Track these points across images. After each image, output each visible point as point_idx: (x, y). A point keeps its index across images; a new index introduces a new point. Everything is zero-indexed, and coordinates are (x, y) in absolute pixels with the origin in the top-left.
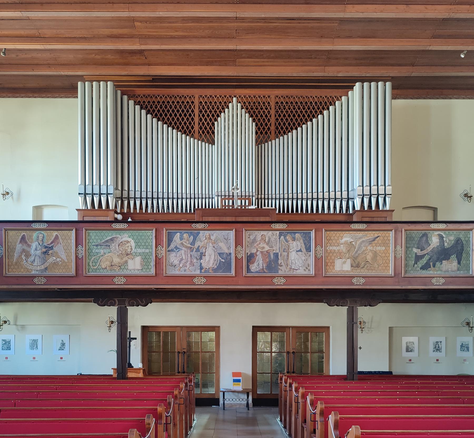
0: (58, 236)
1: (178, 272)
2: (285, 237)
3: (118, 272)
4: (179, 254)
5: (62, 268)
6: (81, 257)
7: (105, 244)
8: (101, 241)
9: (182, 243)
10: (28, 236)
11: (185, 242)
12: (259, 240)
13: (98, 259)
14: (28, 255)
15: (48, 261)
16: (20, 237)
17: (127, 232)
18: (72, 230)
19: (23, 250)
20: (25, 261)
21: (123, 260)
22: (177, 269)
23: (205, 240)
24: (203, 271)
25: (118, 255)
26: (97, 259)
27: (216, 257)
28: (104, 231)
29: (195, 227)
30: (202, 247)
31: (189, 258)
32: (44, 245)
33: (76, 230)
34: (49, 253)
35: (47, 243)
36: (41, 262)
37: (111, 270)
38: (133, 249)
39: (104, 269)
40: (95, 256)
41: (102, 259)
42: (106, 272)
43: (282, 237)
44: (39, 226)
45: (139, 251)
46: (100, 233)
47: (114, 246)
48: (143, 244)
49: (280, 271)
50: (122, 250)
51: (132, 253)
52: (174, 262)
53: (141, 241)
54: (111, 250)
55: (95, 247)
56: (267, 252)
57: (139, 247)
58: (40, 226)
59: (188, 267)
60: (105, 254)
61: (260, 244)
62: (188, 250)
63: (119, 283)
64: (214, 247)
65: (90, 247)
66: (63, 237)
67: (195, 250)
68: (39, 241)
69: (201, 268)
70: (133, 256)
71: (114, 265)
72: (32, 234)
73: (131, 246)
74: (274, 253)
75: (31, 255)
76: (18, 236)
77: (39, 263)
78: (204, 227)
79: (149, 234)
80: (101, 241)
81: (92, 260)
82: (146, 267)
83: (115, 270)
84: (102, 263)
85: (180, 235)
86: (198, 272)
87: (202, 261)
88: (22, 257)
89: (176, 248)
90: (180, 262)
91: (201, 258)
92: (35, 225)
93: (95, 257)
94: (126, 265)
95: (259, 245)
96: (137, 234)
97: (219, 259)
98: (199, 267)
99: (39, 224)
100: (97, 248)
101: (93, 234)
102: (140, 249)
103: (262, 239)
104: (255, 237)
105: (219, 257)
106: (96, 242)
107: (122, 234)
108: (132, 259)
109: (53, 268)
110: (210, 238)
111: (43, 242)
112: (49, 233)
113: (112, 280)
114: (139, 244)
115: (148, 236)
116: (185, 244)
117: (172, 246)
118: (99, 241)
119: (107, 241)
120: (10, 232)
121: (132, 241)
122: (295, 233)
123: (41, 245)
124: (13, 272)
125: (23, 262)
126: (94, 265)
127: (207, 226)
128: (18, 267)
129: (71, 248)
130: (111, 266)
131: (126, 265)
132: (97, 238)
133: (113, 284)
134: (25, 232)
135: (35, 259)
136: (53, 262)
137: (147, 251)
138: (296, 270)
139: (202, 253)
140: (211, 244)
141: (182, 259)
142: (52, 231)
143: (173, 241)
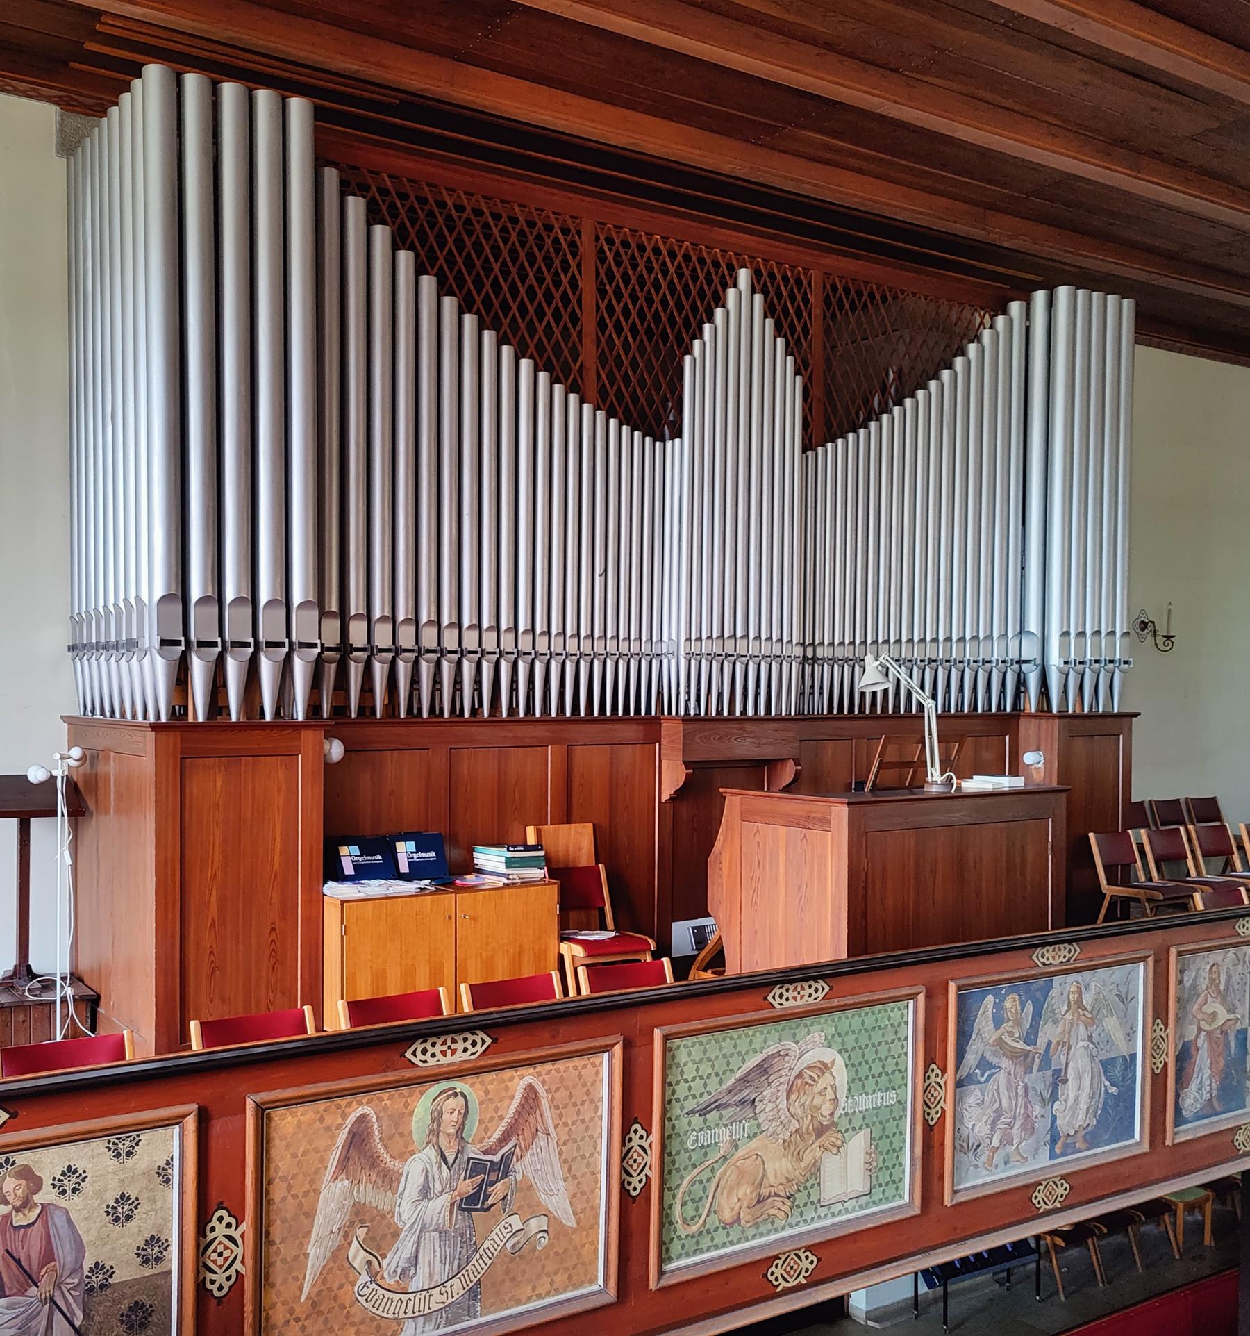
0: (536, 1092)
3: (783, 1228)
6: (639, 1186)
7: (737, 1098)
8: (721, 1082)
9: (1000, 1042)
10: (385, 1123)
11: (1008, 1032)
12: (1204, 987)
13: (709, 1180)
14: (384, 1237)
15: (485, 1246)
16: (342, 1137)
17: (822, 1020)
18: (608, 1048)
19: (357, 1213)
20: (365, 1278)
21: (803, 1165)
22: (984, 1158)
23: (1067, 1012)
25: (785, 1141)
26: (701, 1182)
28: (734, 1034)
29: (1044, 964)
30: (1058, 1043)
32: (465, 1159)
33: (627, 1046)
34: (490, 1201)
35: (481, 1141)
36: (451, 1263)
37: (757, 1225)
38: (842, 1100)
39: (731, 1224)
40: (694, 1166)
41: (724, 1173)
42: (739, 1242)
44: (444, 1053)
45: (865, 1102)
46: (717, 1041)
47: (771, 1098)
48: (877, 1068)
50: (799, 1111)
51: (836, 1119)
52: (976, 1130)
53: (870, 1055)
54: (760, 1121)
55: (697, 1120)
57: (864, 1086)
59: (1016, 1141)
60: (736, 1147)
62: (1018, 1067)
63: (792, 1283)
64: (1090, 1039)
65: (676, 1122)
66: (563, 1094)
67: (1037, 1061)
68: (443, 1141)
69: (1054, 1141)
70: (840, 1136)
72: (406, 1105)
73: (834, 1087)
75: (396, 1235)
76: (328, 1129)
77: (438, 1265)
78: (1068, 956)
79: (892, 1013)
80: (721, 1082)
81: (681, 1190)
82: (884, 1177)
83: (773, 1223)
85: (995, 1003)
86: (1043, 1161)
88: (351, 1255)
89: (984, 1064)
90: (994, 1124)
91: (1054, 1097)
92: (424, 1052)
93: (697, 1171)
95: (1204, 1008)
97: (1103, 1089)
98: (1048, 1136)
99: (444, 1043)
100: (705, 1121)
101: (689, 1052)
102: (867, 1094)
103: (1212, 980)
104: (1195, 979)
105: (1103, 1078)
106: (702, 1094)
107: (801, 1031)
108: (835, 1150)
109: (507, 1283)
110: (1080, 1006)
111: (462, 1138)
112: (492, 1082)
113: (765, 1275)
115: (892, 1025)
116: (1008, 1040)
117: (971, 1059)
118: (713, 1084)
119: (744, 1080)
120: (283, 1117)
121: (840, 1061)
123: (450, 1160)
126: (692, 1213)
127: (1075, 951)
128: (326, 1322)
129: (595, 1145)
130: (759, 1201)
132: (705, 1069)
133: (767, 1293)
134: (369, 1102)
135: (417, 1251)
136: (509, 1246)
137: (891, 1098)
139: (1057, 1072)
140: (1082, 1028)
141: (999, 1113)
142: (507, 1074)
143: (973, 1038)
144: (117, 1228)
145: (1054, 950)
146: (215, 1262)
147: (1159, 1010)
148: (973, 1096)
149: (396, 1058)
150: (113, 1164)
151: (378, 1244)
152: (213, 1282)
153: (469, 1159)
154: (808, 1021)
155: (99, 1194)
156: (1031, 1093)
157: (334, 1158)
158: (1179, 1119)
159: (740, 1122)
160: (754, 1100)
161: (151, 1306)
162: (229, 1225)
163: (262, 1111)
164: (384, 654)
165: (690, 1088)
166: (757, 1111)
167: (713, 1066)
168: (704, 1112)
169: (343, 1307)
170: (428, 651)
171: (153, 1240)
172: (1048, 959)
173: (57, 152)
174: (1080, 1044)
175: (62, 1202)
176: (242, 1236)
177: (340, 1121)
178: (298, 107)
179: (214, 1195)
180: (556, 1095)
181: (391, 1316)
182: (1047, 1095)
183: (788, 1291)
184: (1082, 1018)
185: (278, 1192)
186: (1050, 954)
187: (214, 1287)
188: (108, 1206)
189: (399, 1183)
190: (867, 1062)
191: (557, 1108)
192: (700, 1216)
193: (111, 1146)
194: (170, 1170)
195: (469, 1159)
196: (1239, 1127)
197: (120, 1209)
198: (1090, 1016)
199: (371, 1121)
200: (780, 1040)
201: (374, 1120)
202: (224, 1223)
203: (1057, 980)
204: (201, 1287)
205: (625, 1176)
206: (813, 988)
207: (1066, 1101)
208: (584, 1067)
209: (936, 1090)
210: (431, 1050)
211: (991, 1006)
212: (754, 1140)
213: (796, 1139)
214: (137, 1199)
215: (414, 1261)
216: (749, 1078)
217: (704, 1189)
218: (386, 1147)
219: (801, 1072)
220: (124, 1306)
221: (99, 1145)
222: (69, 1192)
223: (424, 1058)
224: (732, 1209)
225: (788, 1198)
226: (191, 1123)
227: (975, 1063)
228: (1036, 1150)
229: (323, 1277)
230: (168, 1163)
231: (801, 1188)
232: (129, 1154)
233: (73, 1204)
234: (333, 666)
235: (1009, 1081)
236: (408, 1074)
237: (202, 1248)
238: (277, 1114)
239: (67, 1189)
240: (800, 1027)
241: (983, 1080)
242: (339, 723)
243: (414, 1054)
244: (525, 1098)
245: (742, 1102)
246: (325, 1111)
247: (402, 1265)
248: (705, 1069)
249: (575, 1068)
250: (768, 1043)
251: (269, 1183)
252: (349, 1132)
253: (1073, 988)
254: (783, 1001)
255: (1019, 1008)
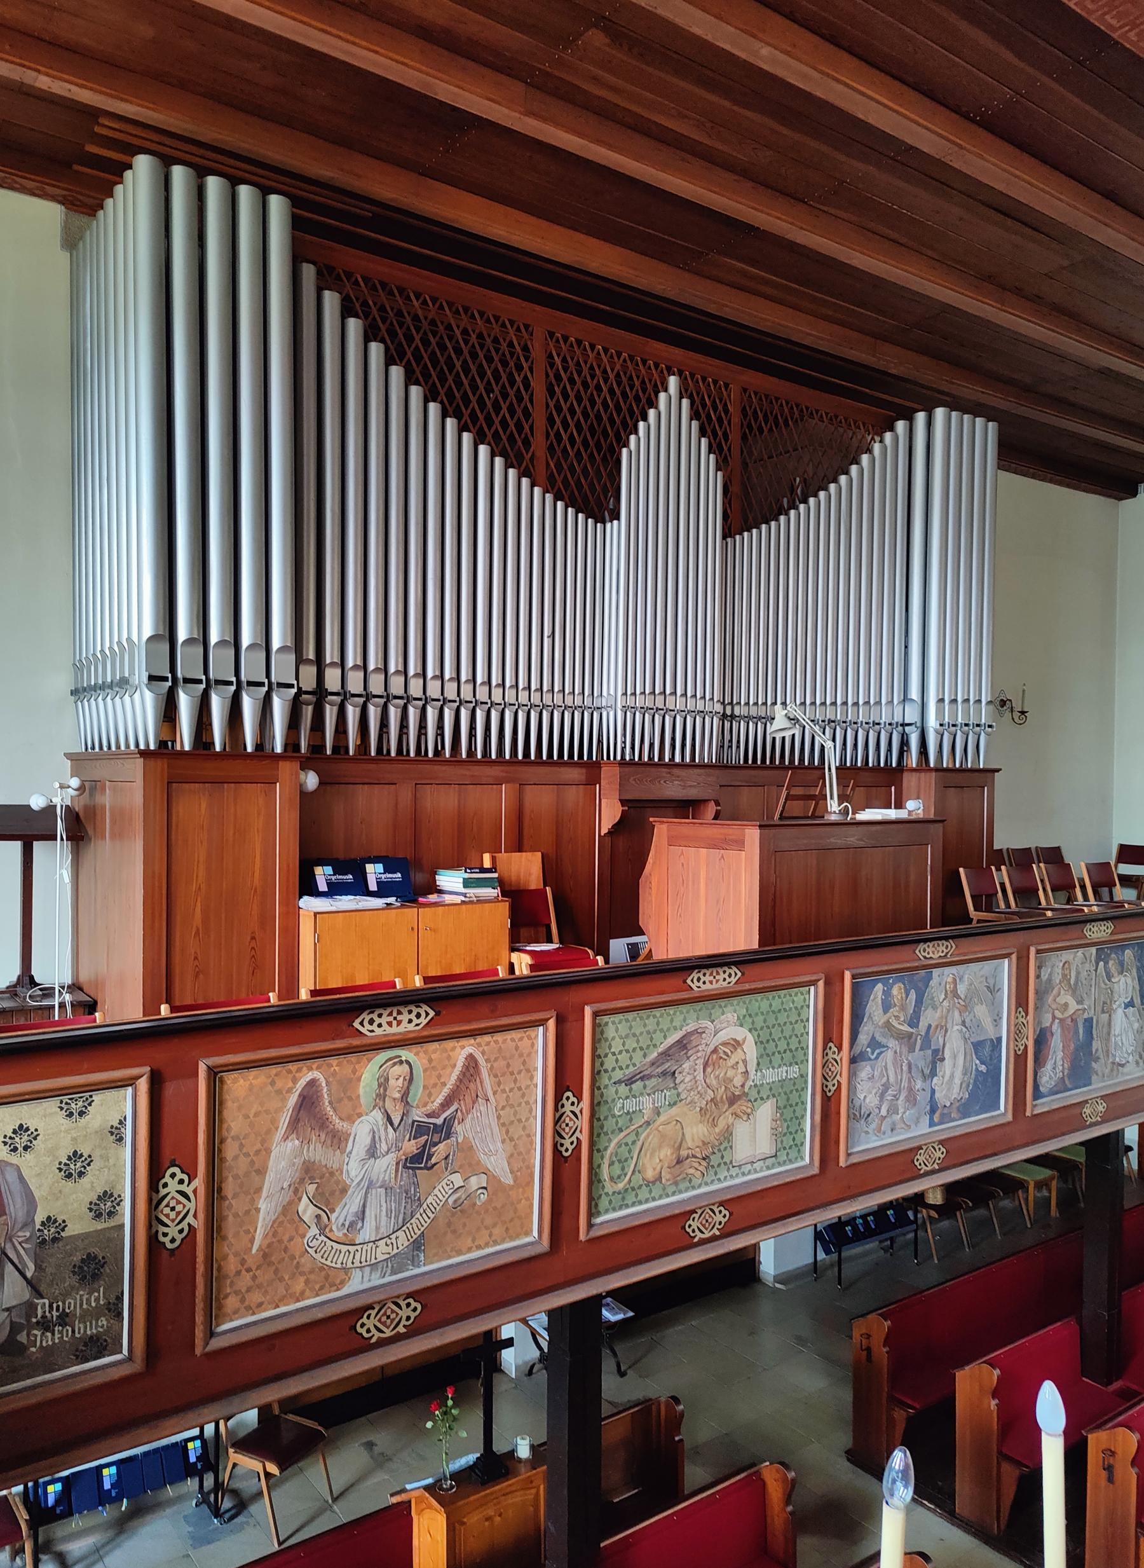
1: (876, 1138)
2: (1106, 963)
3: (700, 1186)
4: (880, 1063)
5: (489, 1221)
6: (571, 1148)
7: (660, 1070)
9: (888, 1024)
12: (1058, 982)
13: (634, 1142)
14: (332, 1193)
15: (429, 1201)
16: (293, 1099)
17: (735, 1002)
18: (543, 1022)
20: (314, 1231)
21: (717, 1130)
22: (874, 1126)
24: (936, 1118)
25: (701, 1109)
26: (626, 1144)
27: (968, 1057)
28: (657, 1012)
29: (925, 957)
30: (937, 1026)
31: (904, 1076)
32: (410, 1121)
33: (560, 1022)
34: (433, 1160)
35: (425, 1105)
36: (397, 1217)
37: (676, 1183)
38: (752, 1072)
39: (654, 1183)
40: (621, 1130)
41: (648, 1136)
42: (660, 1197)
43: (1101, 964)
44: (390, 1024)
45: (771, 1075)
46: (641, 1018)
47: (690, 1070)
48: (782, 1045)
49: (1094, 1077)
50: (714, 1082)
51: (746, 1090)
52: (867, 1100)
54: (680, 1090)
55: (623, 1089)
56: (1072, 1020)
57: (771, 1061)
58: (399, 1023)
59: (901, 1111)
60: (659, 1114)
61: (1059, 994)
63: (707, 1235)
64: (963, 1023)
65: (604, 1091)
66: (502, 1063)
67: (919, 1042)
68: (389, 1104)
69: (933, 1111)
70: (750, 1105)
71: (688, 1157)
72: (354, 1072)
73: (745, 1062)
74: (1086, 1020)
75: (344, 1191)
76: (279, 1092)
77: (384, 1218)
78: (945, 951)
79: (796, 997)
80: (645, 1056)
81: (609, 1152)
82: (788, 1141)
83: (690, 1181)
84: (645, 1160)
86: (924, 1128)
87: (935, 1079)
89: (874, 1044)
90: (882, 1096)
91: (933, 1073)
92: (371, 1022)
93: (622, 1135)
94: (725, 1149)
96: (765, 1005)
98: (928, 1108)
99: (390, 1014)
100: (631, 1090)
101: (616, 1028)
102: (773, 1068)
103: (1064, 976)
104: (1050, 974)
106: (628, 1066)
107: (716, 1012)
108: (745, 1118)
111: (407, 1102)
112: (435, 1052)
113: (684, 1228)
114: (771, 1047)
115: (796, 1008)
116: (895, 1023)
117: (863, 1039)
118: (638, 1057)
119: (666, 1055)
120: (235, 1081)
121: (750, 1039)
122: (1123, 948)
124: (248, 1308)
125: (303, 1236)
126: (618, 1172)
128: (276, 1271)
129: (531, 1111)
130: (679, 1162)
131: (725, 1149)
132: (631, 1044)
134: (317, 1068)
135: (364, 1206)
136: (451, 1201)
137: (793, 1073)
138: (1122, 1066)
139: (936, 1052)
140: (956, 1013)
141: (886, 1087)
142: (449, 1044)
143: (865, 1020)
144: (70, 1184)
145: (934, 946)
146: (167, 1216)
147: (1021, 1001)
148: (865, 1071)
149: (344, 1027)
150: (66, 1123)
151: (327, 1200)
152: (165, 1235)
153: (414, 1121)
154: (722, 1002)
155: (51, 1152)
156: (914, 1070)
157: (284, 1120)
158: (1037, 1095)
159: (662, 1091)
160: (674, 1072)
161: (103, 1258)
162: (181, 1182)
163: (214, 1074)
164: (356, 699)
165: (617, 1061)
166: (677, 1081)
167: (638, 1041)
168: (629, 1081)
169: (293, 1257)
170: (396, 697)
171: (106, 1196)
172: (928, 953)
173: (62, 246)
174: (956, 1028)
175: (14, 1159)
176: (195, 1192)
177: (290, 1084)
178: (276, 202)
179: (167, 1153)
180: (495, 1065)
181: (339, 1266)
182: (927, 1071)
183: (703, 1242)
184: (958, 1005)
185: (230, 1150)
186: (930, 950)
187: (166, 1240)
188: (60, 1163)
189: (347, 1143)
190: (774, 1040)
191: (496, 1076)
192: (625, 1175)
193: (63, 1105)
194: (123, 1130)
195: (414, 1121)
196: (1086, 1102)
197: (72, 1166)
198: (963, 1003)
199: (320, 1085)
200: (698, 1019)
201: (324, 1084)
202: (177, 1179)
203: (936, 972)
204: (153, 1242)
205: (557, 1138)
206: (727, 973)
207: (943, 1077)
208: (521, 1039)
209: (833, 1065)
210: (377, 1021)
211: (880, 994)
212: (674, 1108)
213: (711, 1107)
214: (90, 1156)
215: (362, 1215)
216: (671, 1052)
217: (630, 1151)
218: (335, 1110)
219: (716, 1048)
220: (77, 1258)
221: (52, 1105)
222: (20, 1149)
223: (371, 1028)
224: (654, 1169)
225: (704, 1159)
226: (143, 1084)
227: (866, 1043)
228: (918, 1119)
229: (274, 1231)
230: (121, 1123)
231: (716, 1151)
232: (81, 1114)
233: (26, 1162)
234: (310, 708)
235: (895, 1059)
236: (356, 1042)
237: (154, 1201)
238: (230, 1078)
239: (18, 1146)
240: (716, 1007)
241: (873, 1057)
242: (315, 758)
243: (362, 1023)
244: (466, 1067)
245: (664, 1074)
246: (276, 1075)
247: (350, 1218)
248: (631, 1044)
249: (513, 1040)
250: (687, 1022)
251: (222, 1141)
252: (300, 1095)
253: (950, 979)
254: (701, 984)
255: (904, 996)
